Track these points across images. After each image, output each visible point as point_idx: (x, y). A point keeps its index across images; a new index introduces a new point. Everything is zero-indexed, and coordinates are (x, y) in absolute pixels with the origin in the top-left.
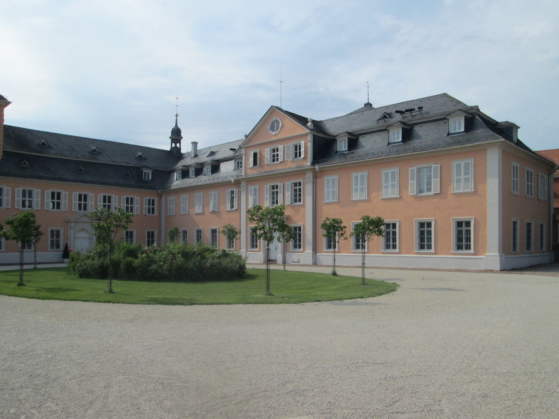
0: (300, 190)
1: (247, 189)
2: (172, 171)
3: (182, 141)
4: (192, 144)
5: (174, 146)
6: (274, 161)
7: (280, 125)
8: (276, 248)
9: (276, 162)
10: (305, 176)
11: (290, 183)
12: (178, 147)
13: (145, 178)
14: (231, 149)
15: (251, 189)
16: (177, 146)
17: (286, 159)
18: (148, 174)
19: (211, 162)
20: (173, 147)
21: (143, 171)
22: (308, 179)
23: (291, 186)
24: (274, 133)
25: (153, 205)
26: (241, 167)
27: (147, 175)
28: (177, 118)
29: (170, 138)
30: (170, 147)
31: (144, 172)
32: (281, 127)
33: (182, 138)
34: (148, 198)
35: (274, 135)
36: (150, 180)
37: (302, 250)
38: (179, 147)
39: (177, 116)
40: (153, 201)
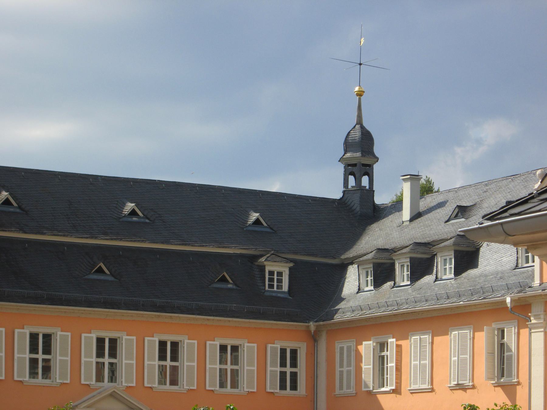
3: (377, 168)
5: (354, 184)
13: (271, 286)
16: (363, 184)
18: (280, 274)
19: (455, 244)
20: (350, 187)
21: (264, 266)
25: (294, 364)
27: (275, 277)
28: (360, 100)
30: (342, 189)
31: (268, 269)
33: (377, 159)
34: (278, 346)
36: (284, 292)
38: (367, 188)
40: (294, 353)
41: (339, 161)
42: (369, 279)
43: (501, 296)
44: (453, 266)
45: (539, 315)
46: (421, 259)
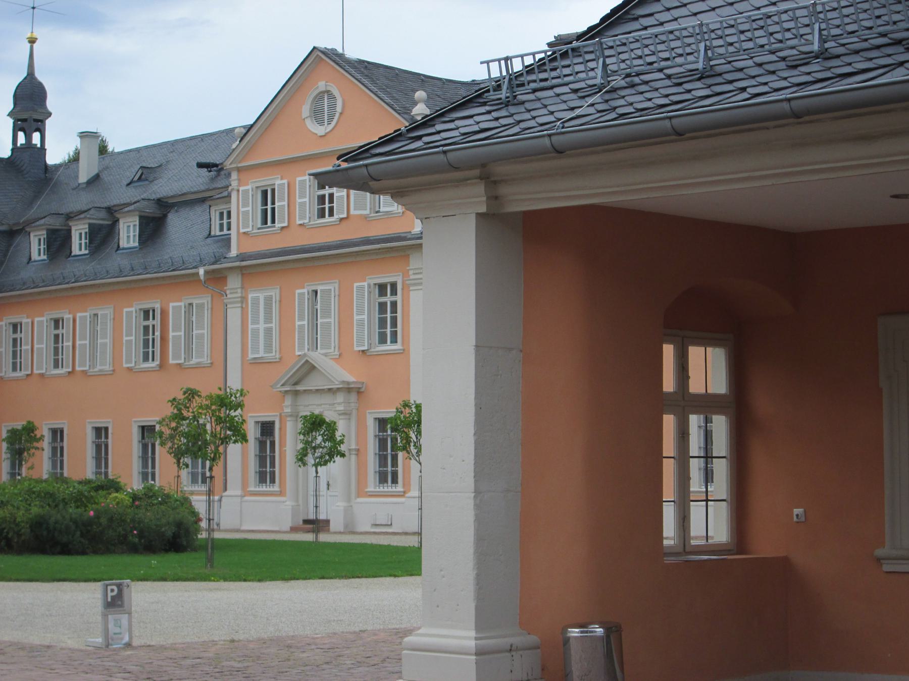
0: (394, 304)
1: (244, 299)
2: (15, 228)
3: (49, 123)
4: (81, 137)
6: (321, 214)
7: (339, 109)
8: (328, 485)
9: (327, 219)
10: (408, 265)
11: (366, 286)
12: (36, 145)
14: (200, 165)
15: (257, 299)
16: (34, 142)
17: (352, 212)
22: (414, 274)
23: (370, 292)
24: (320, 130)
26: (229, 229)
29: (10, 114)
30: (11, 147)
32: (341, 114)
35: (321, 136)
37: (399, 488)
38: (39, 146)
39: (32, 41)
41: (8, 115)
42: (42, 247)
43: (194, 268)
44: (137, 233)
45: (237, 288)
46: (102, 225)
